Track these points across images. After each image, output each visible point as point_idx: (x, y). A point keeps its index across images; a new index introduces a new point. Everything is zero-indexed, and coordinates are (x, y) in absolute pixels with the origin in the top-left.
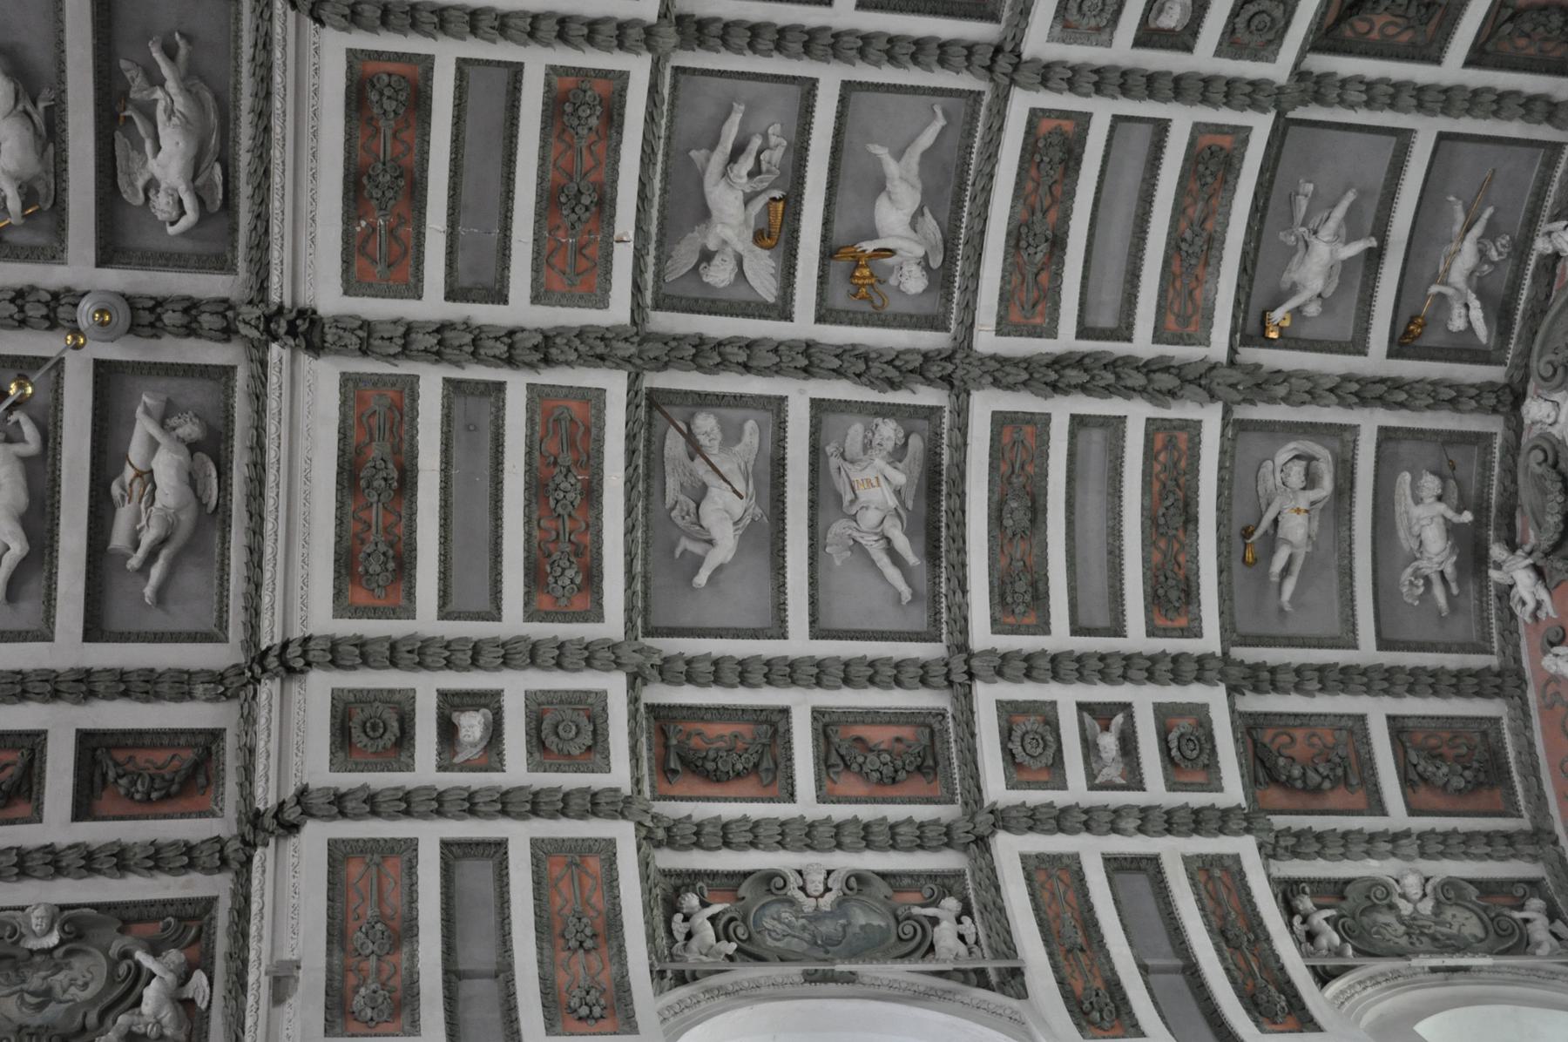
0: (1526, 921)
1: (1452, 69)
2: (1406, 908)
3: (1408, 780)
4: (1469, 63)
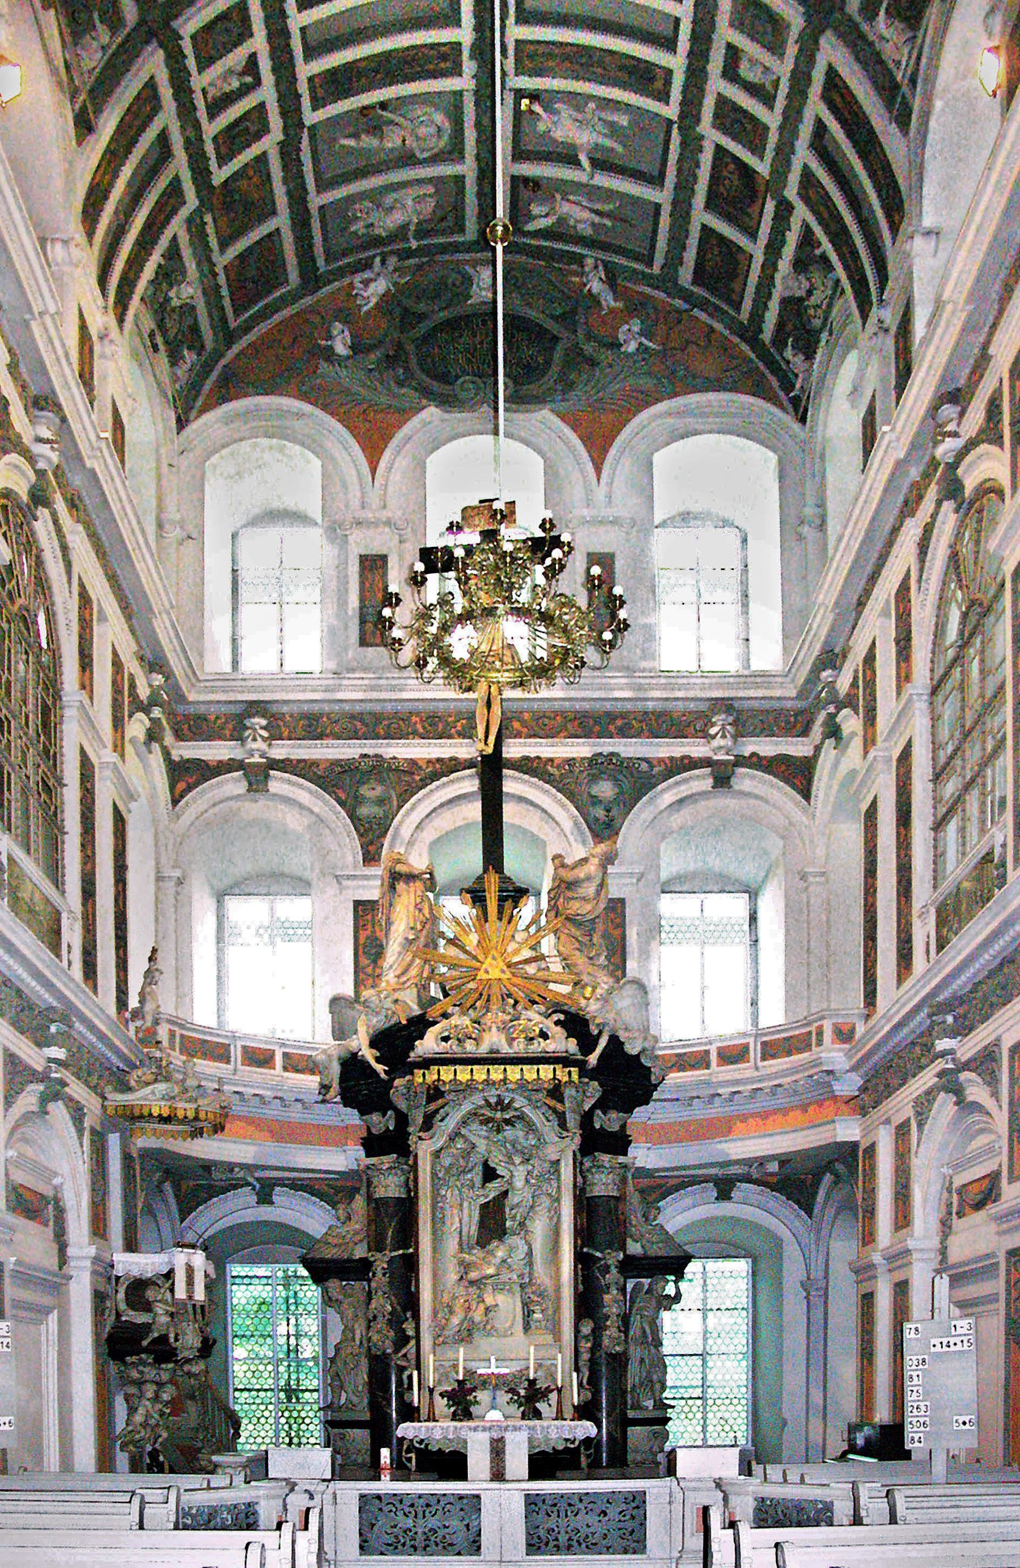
0: (182, 358)
1: (701, 216)
2: (172, 294)
3: (242, 257)
4: (704, 227)
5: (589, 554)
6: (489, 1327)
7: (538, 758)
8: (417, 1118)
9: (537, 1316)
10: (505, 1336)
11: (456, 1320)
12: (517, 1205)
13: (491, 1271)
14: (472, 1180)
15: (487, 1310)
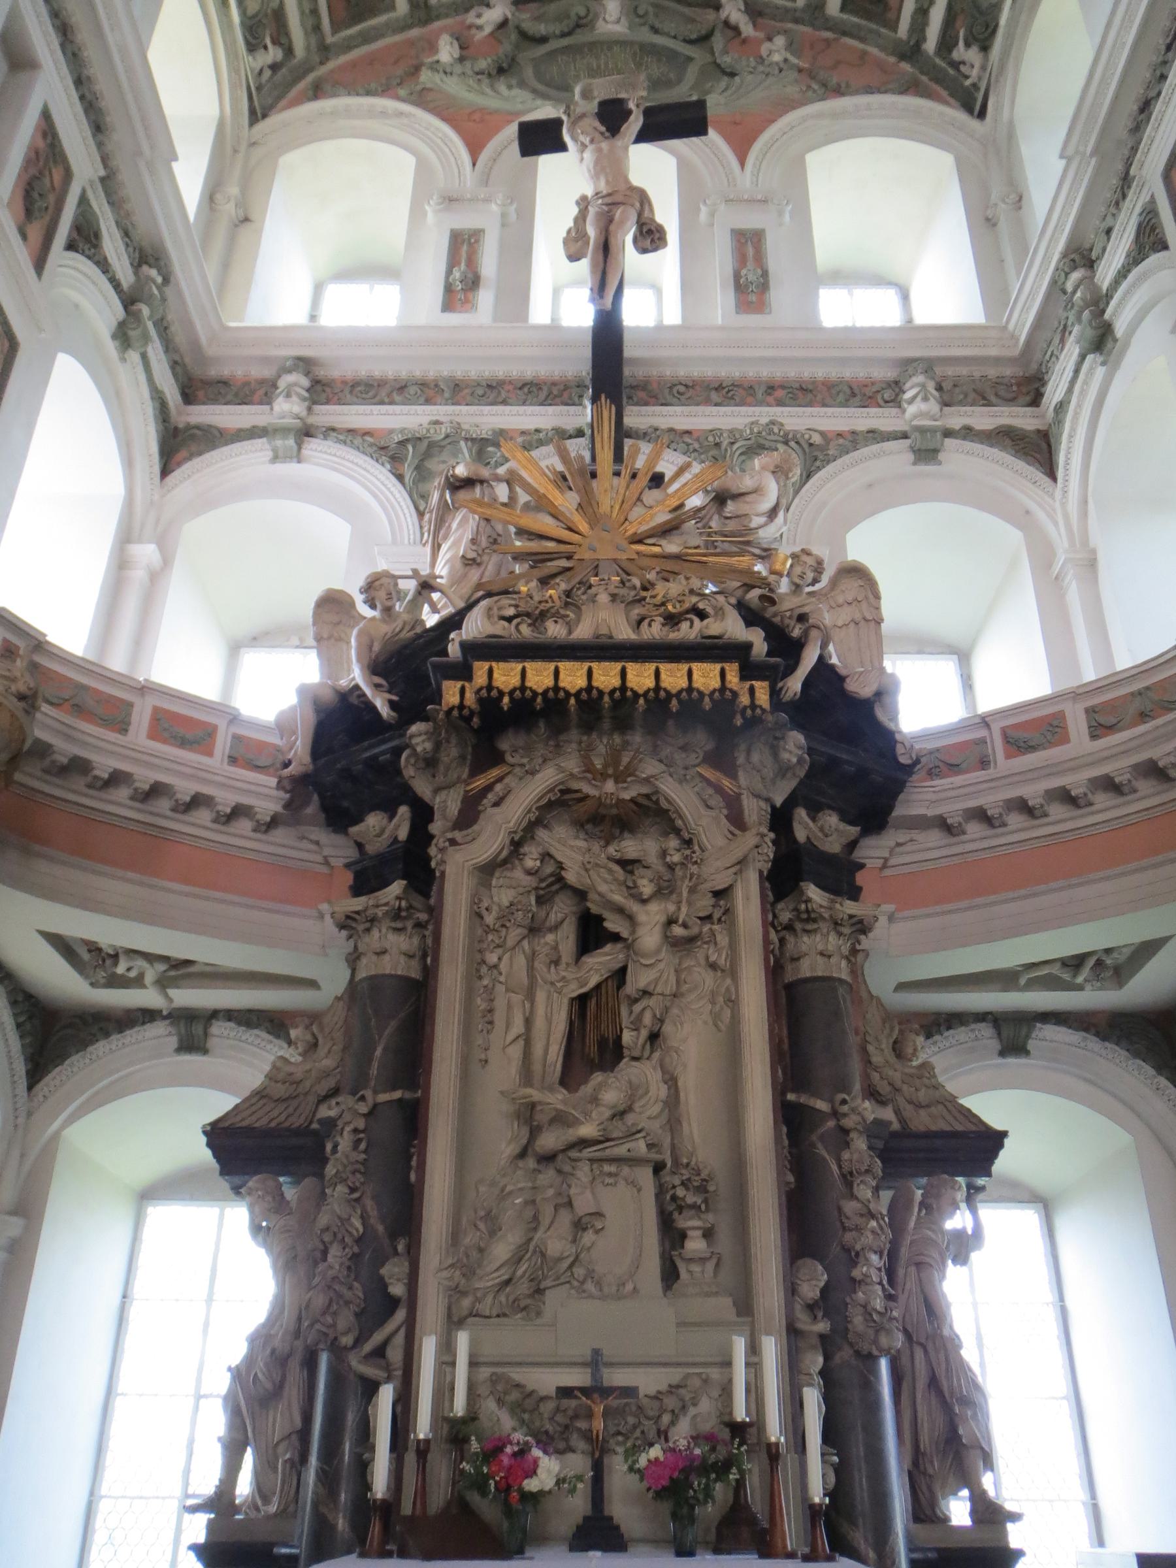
5: (732, 230)
6: (579, 1272)
7: (671, 430)
8: (448, 804)
9: (695, 1245)
10: (619, 1297)
11: (502, 1250)
12: (646, 993)
13: (587, 1130)
14: (555, 948)
15: (579, 1226)
